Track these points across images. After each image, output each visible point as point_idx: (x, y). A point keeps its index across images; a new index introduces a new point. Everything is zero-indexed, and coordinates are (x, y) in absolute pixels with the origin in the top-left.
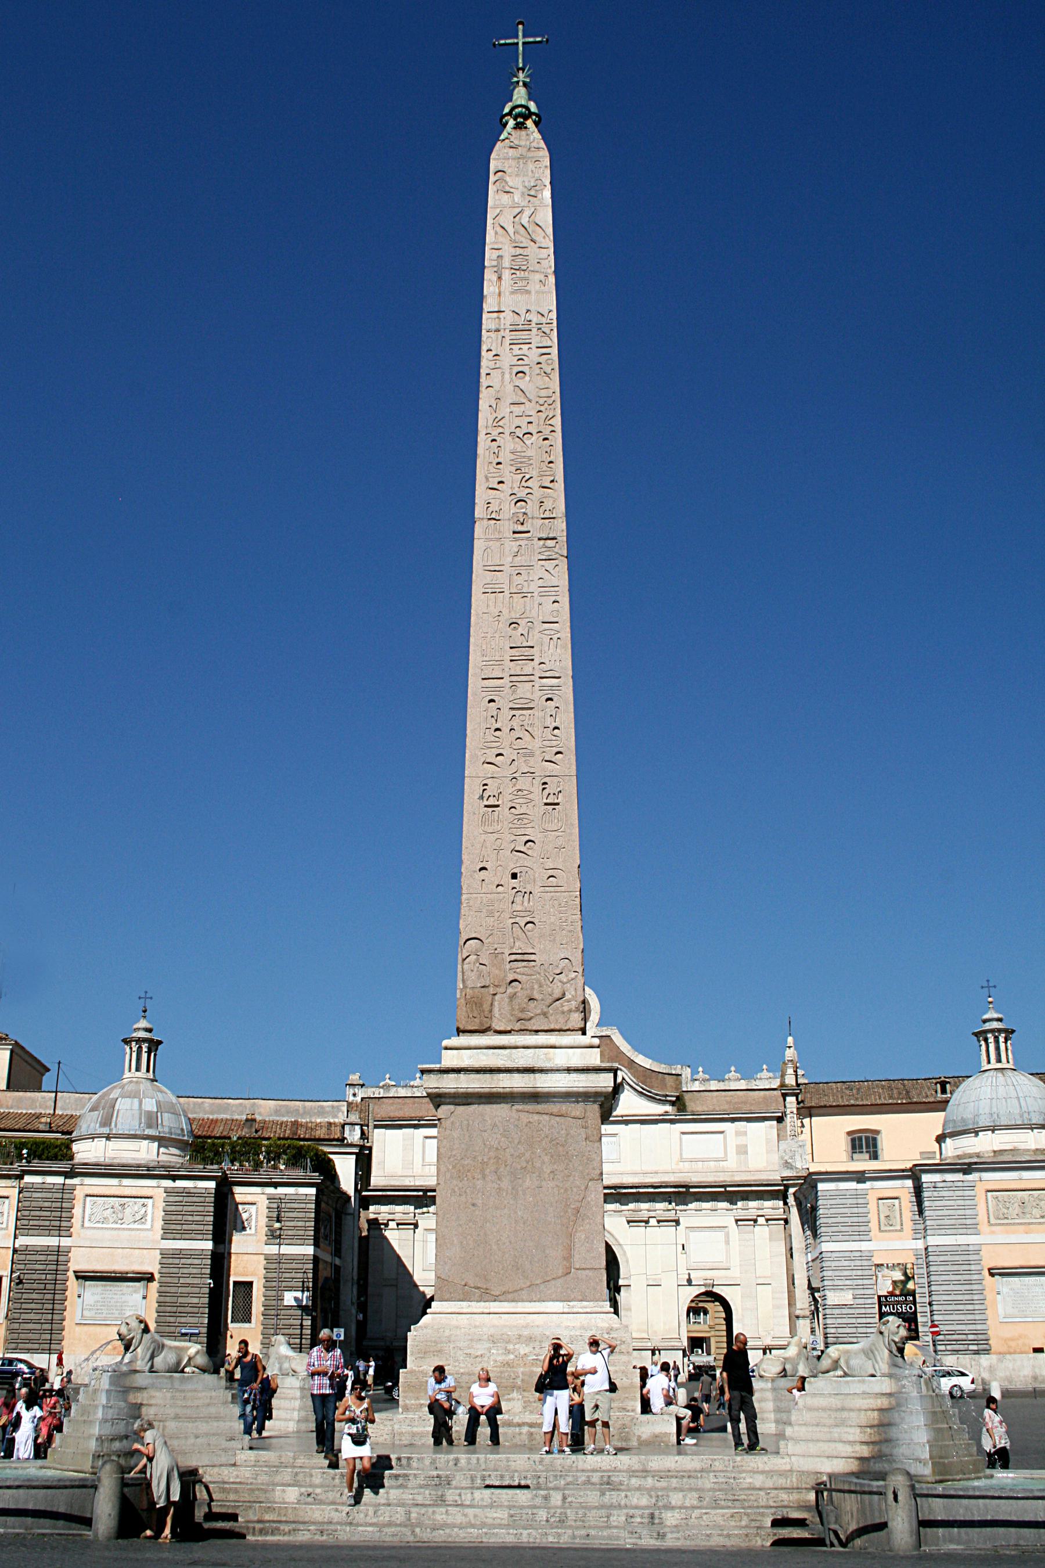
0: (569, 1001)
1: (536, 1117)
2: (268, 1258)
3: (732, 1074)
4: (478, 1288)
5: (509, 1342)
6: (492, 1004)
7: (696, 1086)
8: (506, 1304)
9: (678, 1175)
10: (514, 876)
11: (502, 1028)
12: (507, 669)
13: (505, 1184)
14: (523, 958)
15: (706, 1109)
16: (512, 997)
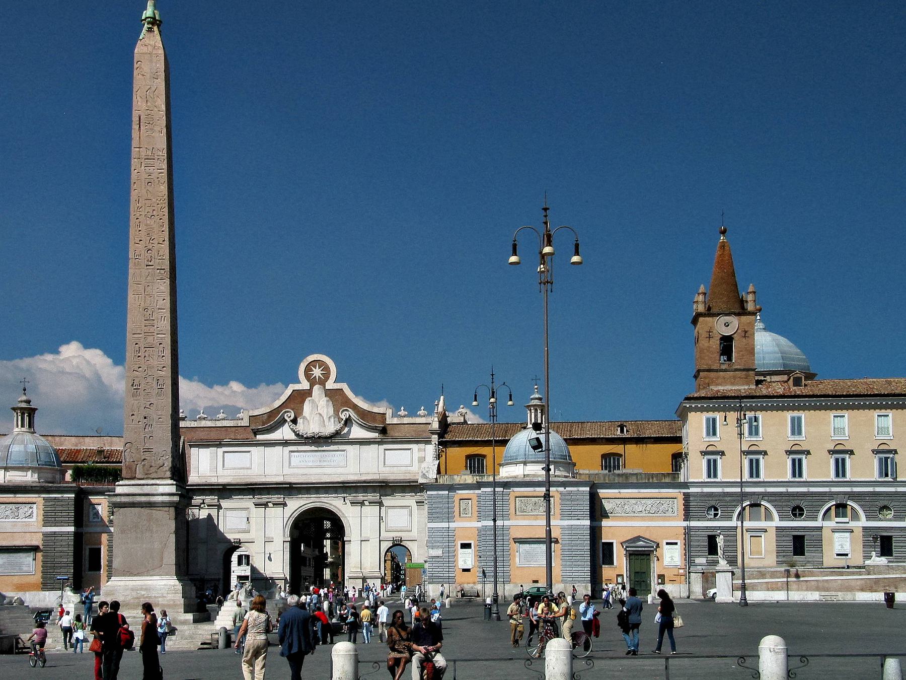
0: (166, 467)
1: (151, 511)
3: (422, 412)
5: (138, 590)
6: (136, 468)
10: (145, 418)
11: (140, 477)
13: (139, 535)
14: (148, 450)
16: (144, 465)
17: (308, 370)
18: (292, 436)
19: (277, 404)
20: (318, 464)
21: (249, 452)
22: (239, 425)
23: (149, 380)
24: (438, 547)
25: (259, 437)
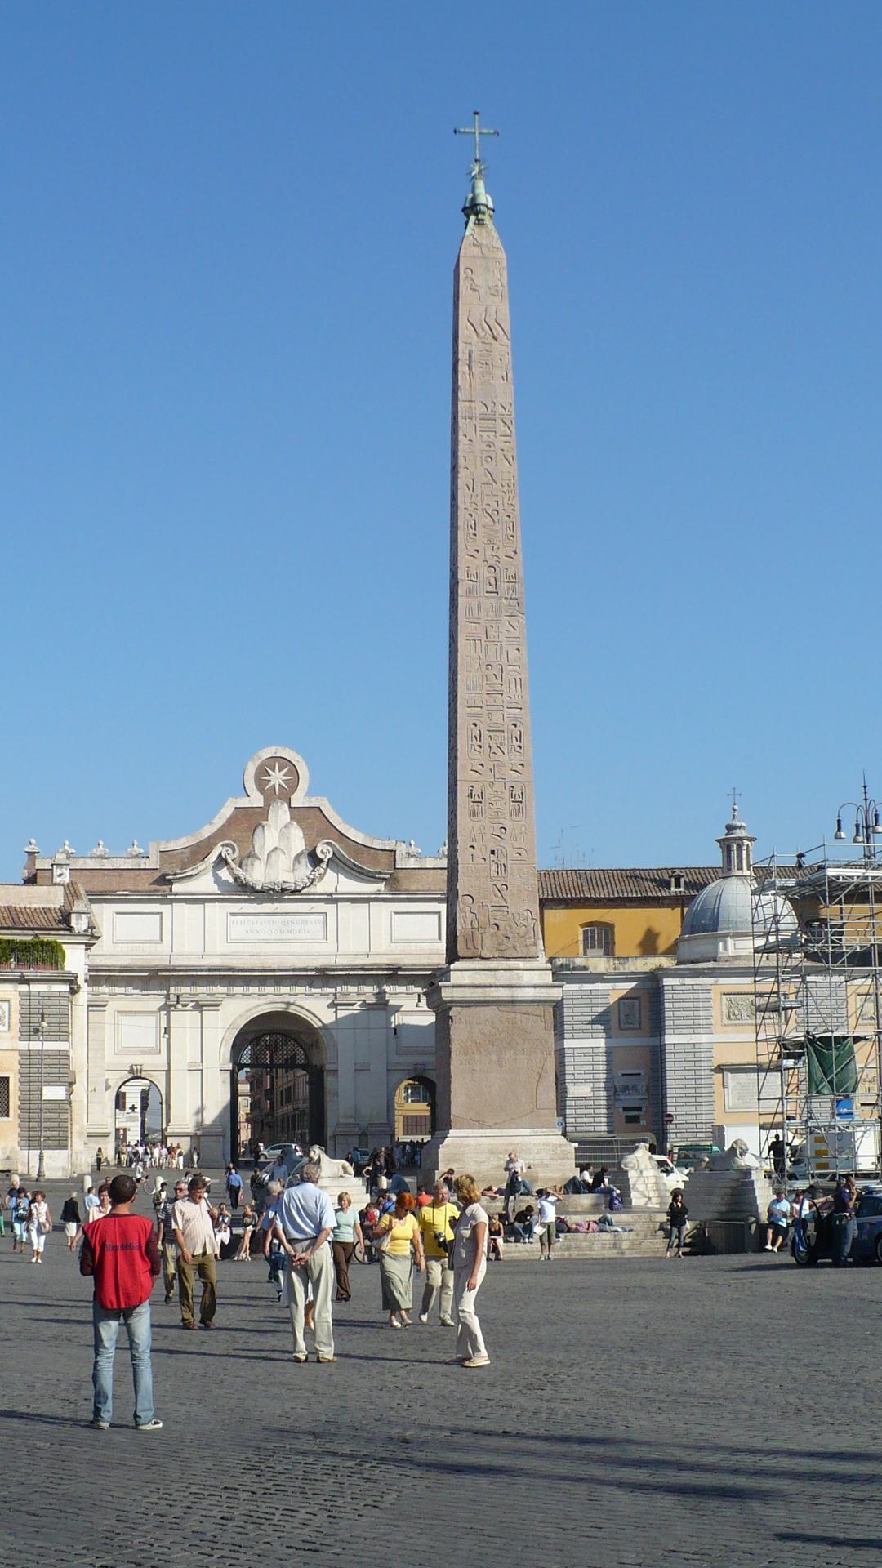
1: (513, 1015)
2: (21, 1053)
4: (478, 1121)
7: (412, 863)
8: (496, 1131)
9: (389, 956)
10: (493, 852)
12: (485, 701)
13: (494, 1057)
14: (499, 909)
15: (421, 888)
17: (262, 773)
18: (215, 888)
19: (207, 832)
20: (279, 936)
21: (161, 914)
22: (142, 867)
23: (498, 786)
24: (585, 1081)
25: (176, 888)
